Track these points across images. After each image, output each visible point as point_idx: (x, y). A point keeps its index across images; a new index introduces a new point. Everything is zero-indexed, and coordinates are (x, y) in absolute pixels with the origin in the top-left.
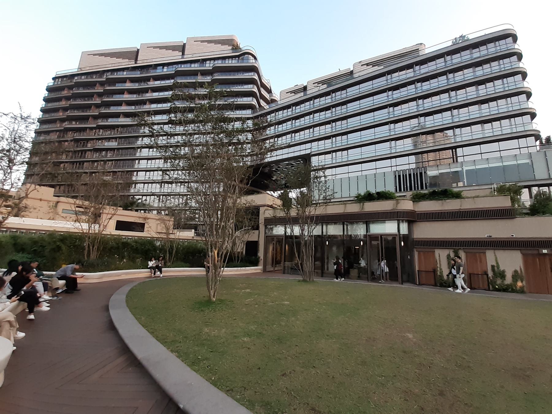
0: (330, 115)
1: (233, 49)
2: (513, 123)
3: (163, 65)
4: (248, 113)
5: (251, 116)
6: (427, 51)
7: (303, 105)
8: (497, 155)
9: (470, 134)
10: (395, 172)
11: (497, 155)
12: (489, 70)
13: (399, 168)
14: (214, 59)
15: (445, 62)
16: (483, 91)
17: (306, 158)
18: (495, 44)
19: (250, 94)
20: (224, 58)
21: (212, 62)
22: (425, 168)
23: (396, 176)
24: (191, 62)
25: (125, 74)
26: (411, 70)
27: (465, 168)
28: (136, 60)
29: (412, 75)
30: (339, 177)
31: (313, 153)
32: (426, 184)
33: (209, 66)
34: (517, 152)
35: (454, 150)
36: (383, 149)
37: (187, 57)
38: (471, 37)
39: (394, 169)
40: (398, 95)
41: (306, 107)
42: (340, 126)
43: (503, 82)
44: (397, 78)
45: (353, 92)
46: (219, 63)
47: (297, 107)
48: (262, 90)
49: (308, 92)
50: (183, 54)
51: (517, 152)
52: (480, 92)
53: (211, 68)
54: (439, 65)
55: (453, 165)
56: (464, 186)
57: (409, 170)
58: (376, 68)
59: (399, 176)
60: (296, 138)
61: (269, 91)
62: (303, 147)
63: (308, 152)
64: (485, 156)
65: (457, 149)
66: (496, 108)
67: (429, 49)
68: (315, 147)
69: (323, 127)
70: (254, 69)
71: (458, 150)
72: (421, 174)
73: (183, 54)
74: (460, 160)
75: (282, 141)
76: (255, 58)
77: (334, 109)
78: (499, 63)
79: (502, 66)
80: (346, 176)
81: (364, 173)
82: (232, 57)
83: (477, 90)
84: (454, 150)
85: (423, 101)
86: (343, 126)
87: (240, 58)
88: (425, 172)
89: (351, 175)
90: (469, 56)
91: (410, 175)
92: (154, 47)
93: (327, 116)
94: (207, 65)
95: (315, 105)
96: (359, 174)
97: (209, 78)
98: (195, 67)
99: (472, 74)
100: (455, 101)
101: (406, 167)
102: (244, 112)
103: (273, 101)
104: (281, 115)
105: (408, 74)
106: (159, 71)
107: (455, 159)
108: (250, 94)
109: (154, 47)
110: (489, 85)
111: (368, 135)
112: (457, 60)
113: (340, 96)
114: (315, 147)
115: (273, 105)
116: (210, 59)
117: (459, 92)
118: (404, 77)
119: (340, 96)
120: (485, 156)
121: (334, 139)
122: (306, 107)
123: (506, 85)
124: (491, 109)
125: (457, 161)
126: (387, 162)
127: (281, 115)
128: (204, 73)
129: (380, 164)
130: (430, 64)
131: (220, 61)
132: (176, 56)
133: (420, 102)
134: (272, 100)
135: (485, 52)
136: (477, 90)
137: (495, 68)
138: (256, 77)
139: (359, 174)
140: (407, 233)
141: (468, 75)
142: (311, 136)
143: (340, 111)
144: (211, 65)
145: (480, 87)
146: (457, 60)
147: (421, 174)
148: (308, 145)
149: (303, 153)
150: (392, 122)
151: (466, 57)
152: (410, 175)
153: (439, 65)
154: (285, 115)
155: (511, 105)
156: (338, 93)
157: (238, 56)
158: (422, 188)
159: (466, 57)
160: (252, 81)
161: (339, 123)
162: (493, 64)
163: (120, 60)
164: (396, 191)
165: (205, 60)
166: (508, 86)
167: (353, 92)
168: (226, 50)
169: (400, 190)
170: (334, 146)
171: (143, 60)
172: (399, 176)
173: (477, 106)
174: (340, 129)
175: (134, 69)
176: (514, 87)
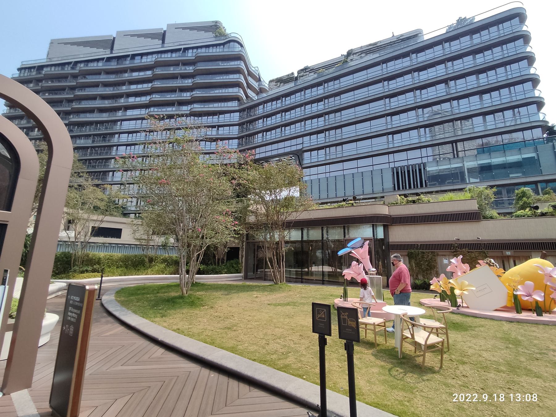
0: (322, 107)
1: (216, 36)
3: (142, 55)
4: (233, 105)
5: (237, 108)
6: (426, 37)
7: (293, 96)
10: (393, 169)
12: (491, 57)
13: (397, 164)
14: (197, 48)
15: (443, 49)
16: (484, 80)
17: (298, 155)
19: (237, 85)
20: (208, 46)
21: (195, 51)
22: (424, 165)
23: (394, 173)
25: (100, 65)
26: (408, 58)
28: (112, 49)
29: (408, 64)
30: (332, 174)
31: (305, 149)
32: (425, 181)
33: (190, 55)
35: (454, 144)
36: (380, 144)
39: (392, 165)
40: (394, 85)
41: (298, 98)
42: (333, 119)
44: (393, 67)
45: (346, 82)
46: (203, 52)
47: (287, 99)
48: (250, 79)
50: (163, 42)
52: (481, 81)
53: (194, 58)
54: (437, 52)
55: (453, 161)
57: (408, 167)
59: (397, 173)
60: (286, 132)
61: (259, 80)
62: (294, 142)
63: (300, 147)
66: (499, 99)
67: (428, 35)
68: (307, 142)
69: (315, 120)
70: (239, 58)
71: (460, 146)
72: (420, 170)
73: (163, 42)
74: (461, 154)
75: (270, 136)
76: (242, 46)
77: (326, 101)
80: (341, 173)
81: (360, 170)
82: (216, 45)
83: (478, 78)
84: (454, 144)
85: (421, 92)
86: (336, 119)
87: (225, 46)
88: (424, 169)
89: (346, 172)
91: (409, 171)
92: (132, 36)
93: (319, 107)
94: (190, 55)
95: (306, 96)
96: (355, 171)
97: (191, 68)
98: (175, 57)
99: (472, 62)
100: (454, 91)
101: (405, 163)
103: (262, 90)
104: (270, 107)
105: (405, 63)
106: (138, 62)
107: (456, 155)
108: (237, 85)
109: (132, 36)
110: (491, 73)
111: (363, 129)
112: (456, 47)
113: (332, 87)
114: (307, 142)
115: (264, 95)
116: (193, 48)
117: (458, 82)
118: (400, 66)
119: (332, 87)
121: (327, 132)
122: (298, 98)
124: (493, 100)
126: (384, 159)
127: (270, 107)
130: (428, 51)
131: (203, 50)
132: (156, 45)
133: (418, 92)
134: (260, 89)
135: (487, 37)
136: (478, 78)
137: (497, 54)
138: (243, 66)
139: (355, 171)
140: (383, 237)
141: (468, 63)
142: (302, 130)
143: (333, 103)
144: (194, 54)
145: (481, 76)
146: (456, 47)
147: (420, 170)
148: (300, 140)
149: (294, 148)
150: (388, 115)
151: (465, 43)
152: (409, 171)
153: (437, 52)
154: (274, 107)
155: (514, 95)
156: (331, 83)
157: (223, 44)
158: (422, 186)
159: (465, 43)
160: (238, 71)
161: (332, 116)
162: (495, 50)
163: (95, 50)
164: (395, 189)
165: (186, 49)
167: (346, 82)
169: (399, 188)
170: (327, 141)
171: (118, 51)
172: (397, 173)
174: (334, 122)
175: (109, 59)
176: (519, 74)
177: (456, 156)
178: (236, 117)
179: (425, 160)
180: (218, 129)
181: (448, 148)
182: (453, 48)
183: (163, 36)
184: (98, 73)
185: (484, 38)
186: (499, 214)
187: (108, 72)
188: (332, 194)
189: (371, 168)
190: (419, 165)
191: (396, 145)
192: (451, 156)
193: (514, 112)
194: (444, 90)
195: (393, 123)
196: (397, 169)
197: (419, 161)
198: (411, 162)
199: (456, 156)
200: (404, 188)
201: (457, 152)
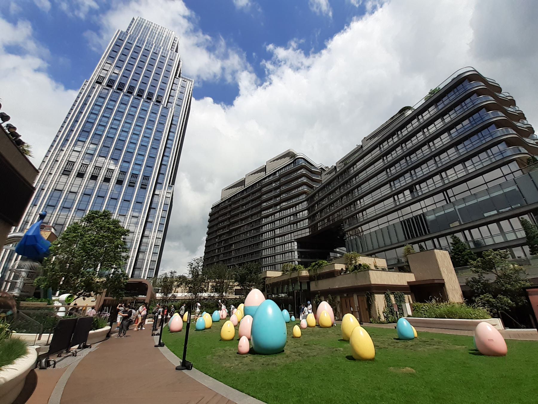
1: (290, 158)
2: (490, 154)
4: (304, 196)
8: (485, 187)
9: (455, 174)
10: (401, 222)
11: (485, 187)
13: (406, 218)
18: (454, 91)
24: (269, 176)
25: (240, 197)
27: (457, 208)
34: (503, 180)
37: (268, 173)
38: (441, 87)
39: (401, 219)
43: (470, 120)
49: (338, 170)
51: (503, 180)
56: (461, 225)
57: (412, 219)
58: (376, 139)
64: (473, 191)
65: (448, 191)
71: (449, 191)
74: (452, 200)
78: (462, 105)
79: (465, 107)
89: (372, 230)
90: (417, 123)
94: (277, 175)
96: (377, 228)
101: (411, 216)
102: (301, 197)
116: (278, 171)
120: (473, 191)
123: (473, 122)
125: (450, 202)
126: (395, 215)
128: (275, 181)
129: (390, 217)
132: (262, 175)
138: (303, 171)
163: (238, 188)
165: (275, 173)
166: (475, 123)
168: (287, 161)
169: (409, 238)
171: (248, 184)
173: (453, 148)
175: (243, 191)
177: (449, 202)
178: (305, 204)
179: (425, 210)
180: (297, 215)
181: (441, 196)
182: (425, 118)
183: (264, 169)
184: (238, 201)
185: (409, 130)
186: (493, 249)
187: (243, 198)
188: (376, 246)
189: (387, 224)
190: (420, 215)
191: (451, 180)
192: (444, 203)
193: (487, 153)
194: (448, 138)
195: (417, 174)
196: (404, 221)
197: (420, 212)
198: (415, 214)
199: (449, 202)
200: (413, 237)
201: (449, 198)
